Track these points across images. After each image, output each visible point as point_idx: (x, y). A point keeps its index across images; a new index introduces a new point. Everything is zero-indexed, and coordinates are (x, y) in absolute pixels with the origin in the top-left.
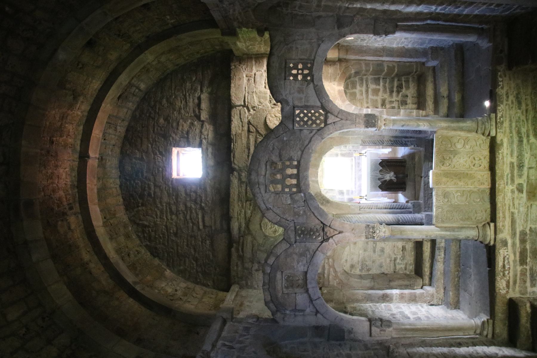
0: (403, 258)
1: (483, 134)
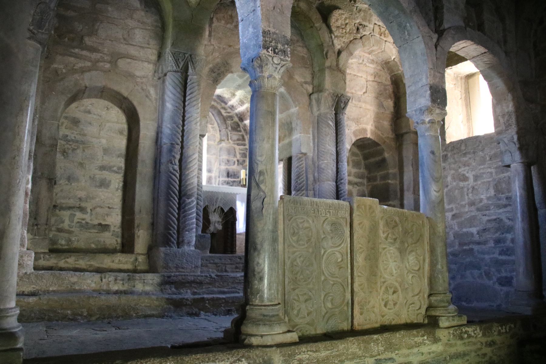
0: (85, 226)
1: (430, 307)
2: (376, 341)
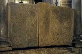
1: (74, 40)
2: (44, 51)
